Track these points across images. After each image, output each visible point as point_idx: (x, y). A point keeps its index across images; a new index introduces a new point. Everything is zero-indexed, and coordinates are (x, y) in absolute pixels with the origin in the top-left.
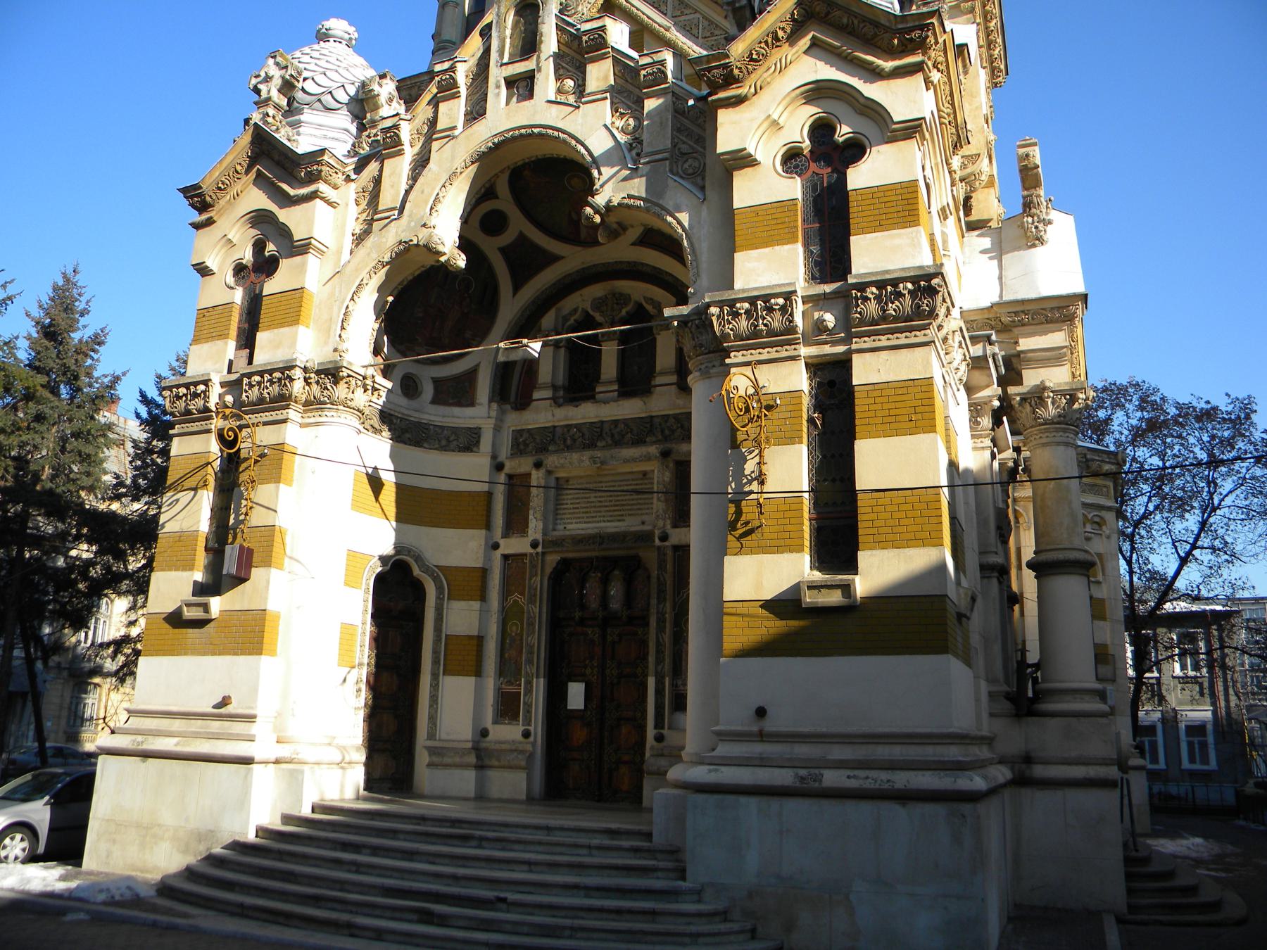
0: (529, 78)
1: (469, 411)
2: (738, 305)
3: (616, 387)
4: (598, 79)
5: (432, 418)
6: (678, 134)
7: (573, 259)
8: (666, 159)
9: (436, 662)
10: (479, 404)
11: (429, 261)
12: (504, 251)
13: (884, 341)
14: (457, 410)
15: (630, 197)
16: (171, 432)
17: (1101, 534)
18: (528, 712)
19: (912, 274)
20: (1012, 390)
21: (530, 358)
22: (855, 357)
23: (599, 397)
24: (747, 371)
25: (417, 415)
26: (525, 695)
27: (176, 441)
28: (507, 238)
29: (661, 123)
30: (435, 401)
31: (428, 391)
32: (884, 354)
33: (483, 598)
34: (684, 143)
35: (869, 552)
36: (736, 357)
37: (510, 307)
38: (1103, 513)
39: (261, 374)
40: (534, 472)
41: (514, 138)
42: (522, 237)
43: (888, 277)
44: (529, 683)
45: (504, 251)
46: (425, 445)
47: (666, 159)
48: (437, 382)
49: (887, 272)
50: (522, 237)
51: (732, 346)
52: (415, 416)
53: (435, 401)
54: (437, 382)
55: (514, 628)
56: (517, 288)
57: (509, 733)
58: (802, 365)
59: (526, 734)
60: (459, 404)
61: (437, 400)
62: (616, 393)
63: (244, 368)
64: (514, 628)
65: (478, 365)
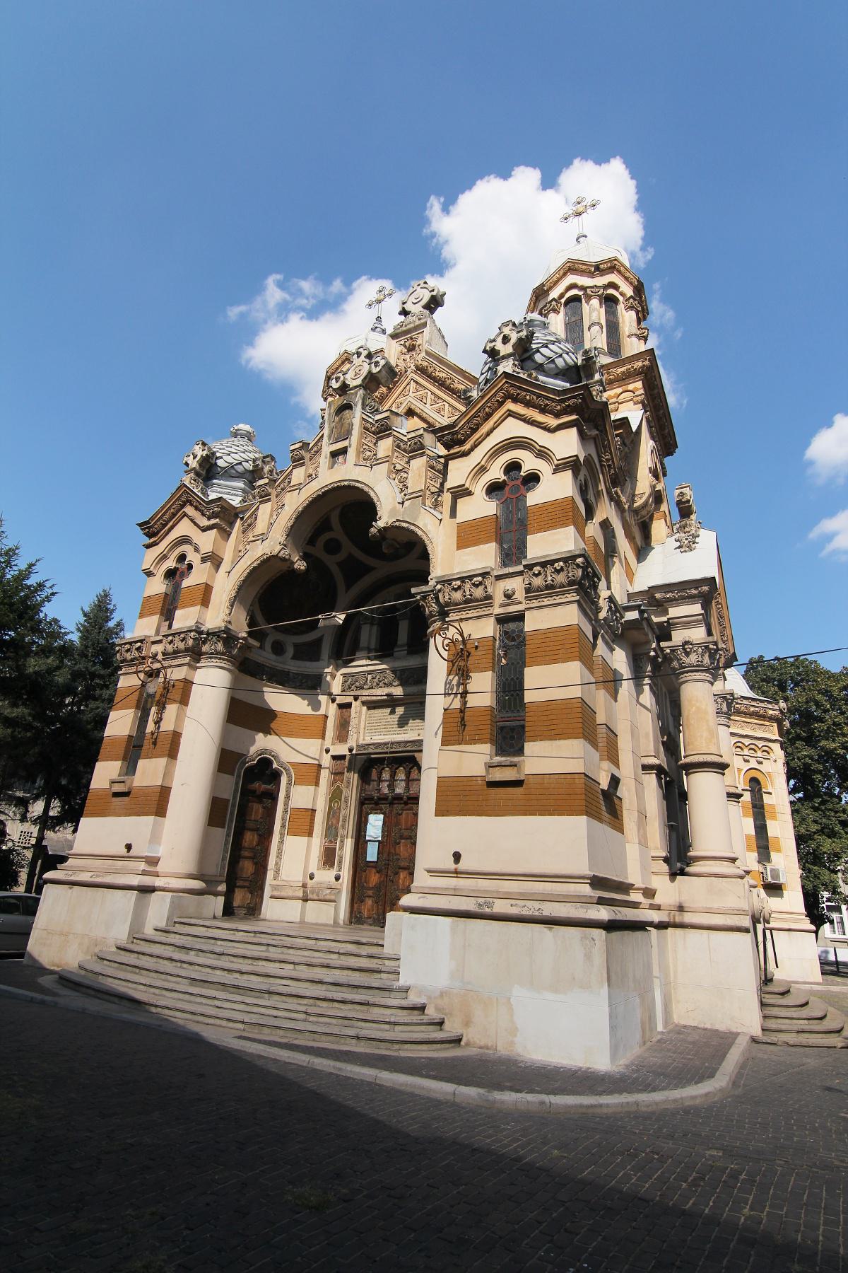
0: (344, 451)
1: (315, 664)
2: (454, 583)
3: (406, 648)
4: (384, 450)
5: (292, 668)
6: (430, 481)
7: (382, 569)
8: (420, 496)
9: (283, 826)
10: (322, 660)
11: (285, 567)
12: (340, 564)
13: (546, 602)
14: (308, 664)
15: (398, 520)
16: (119, 673)
17: (769, 759)
18: (340, 862)
19: (564, 556)
20: (663, 644)
21: (337, 624)
22: (527, 614)
23: (396, 654)
24: (456, 625)
25: (281, 665)
26: (339, 850)
27: (122, 678)
28: (341, 556)
29: (419, 475)
30: (294, 657)
31: (290, 651)
32: (546, 611)
33: (317, 784)
34: (434, 486)
35: (532, 743)
36: (453, 617)
37: (344, 597)
38: (770, 744)
39: (173, 635)
40: (354, 703)
41: (333, 489)
42: (350, 556)
43: (548, 559)
44: (342, 841)
45: (340, 564)
46: (286, 685)
47: (420, 496)
48: (296, 646)
49: (547, 556)
50: (350, 556)
51: (450, 610)
52: (280, 666)
53: (294, 657)
54: (296, 646)
55: (336, 804)
56: (348, 587)
57: (326, 876)
58: (492, 619)
59: (337, 878)
60: (311, 660)
61: (296, 657)
62: (406, 652)
63: (165, 632)
64: (336, 804)
65: (323, 636)
